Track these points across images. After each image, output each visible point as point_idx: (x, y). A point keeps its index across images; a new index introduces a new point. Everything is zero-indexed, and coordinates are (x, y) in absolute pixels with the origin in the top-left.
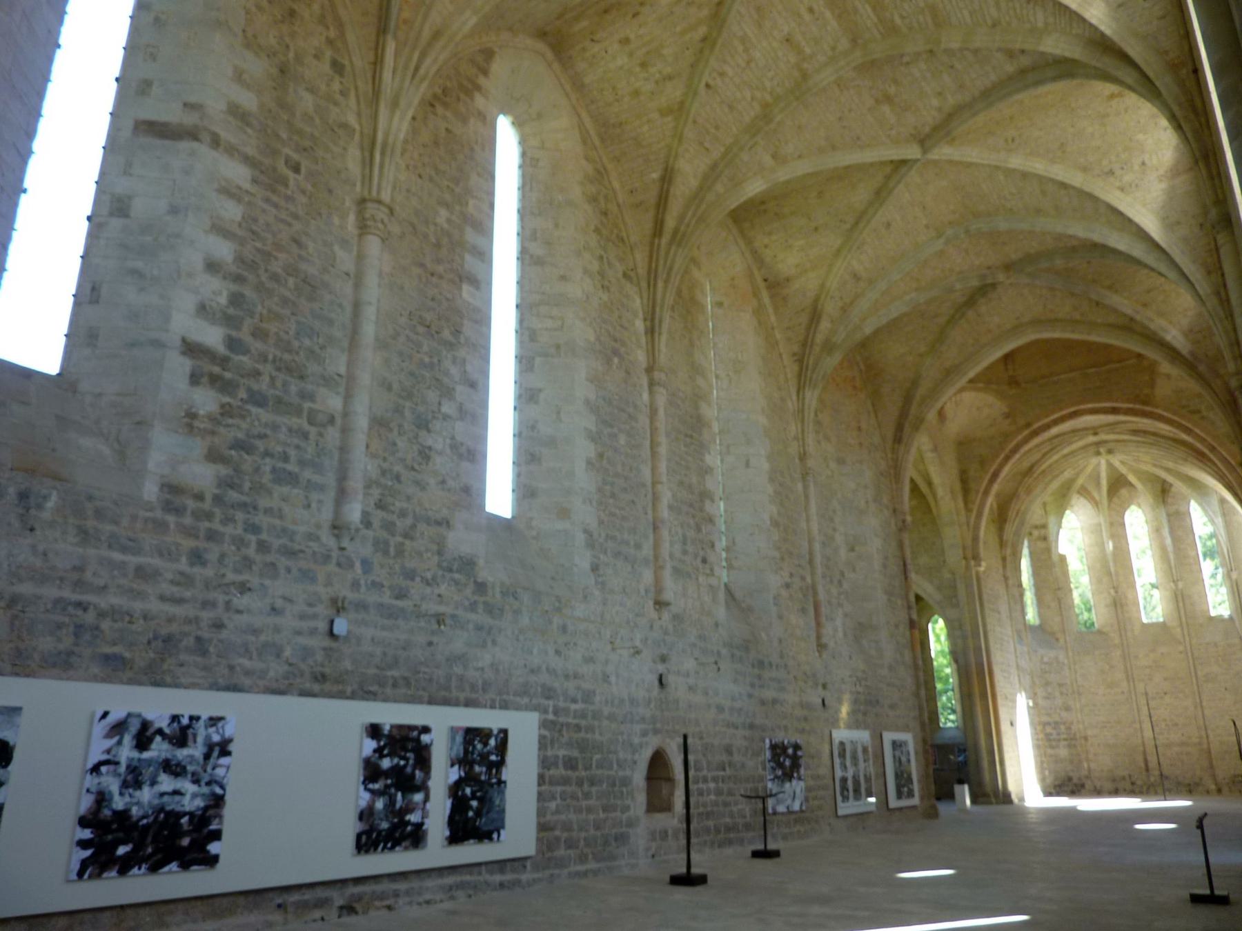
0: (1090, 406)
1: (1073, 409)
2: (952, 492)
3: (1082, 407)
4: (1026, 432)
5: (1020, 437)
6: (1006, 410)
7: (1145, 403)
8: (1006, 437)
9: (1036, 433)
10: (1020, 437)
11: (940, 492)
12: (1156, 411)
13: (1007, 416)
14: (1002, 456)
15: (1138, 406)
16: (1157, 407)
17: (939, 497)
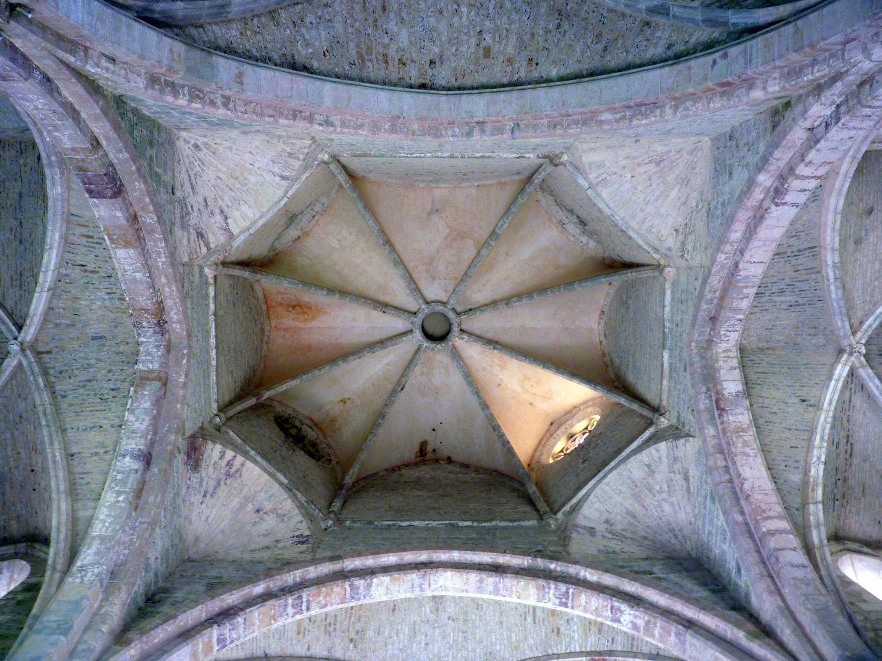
0: (456, 556)
1: (423, 556)
2: (113, 574)
3: (443, 556)
4: (326, 568)
5: (312, 572)
6: (307, 533)
7: (553, 558)
8: (287, 565)
9: (343, 575)
10: (312, 572)
11: (87, 555)
12: (573, 569)
13: (302, 540)
14: (259, 589)
15: (540, 563)
16: (576, 563)
17: (79, 563)
